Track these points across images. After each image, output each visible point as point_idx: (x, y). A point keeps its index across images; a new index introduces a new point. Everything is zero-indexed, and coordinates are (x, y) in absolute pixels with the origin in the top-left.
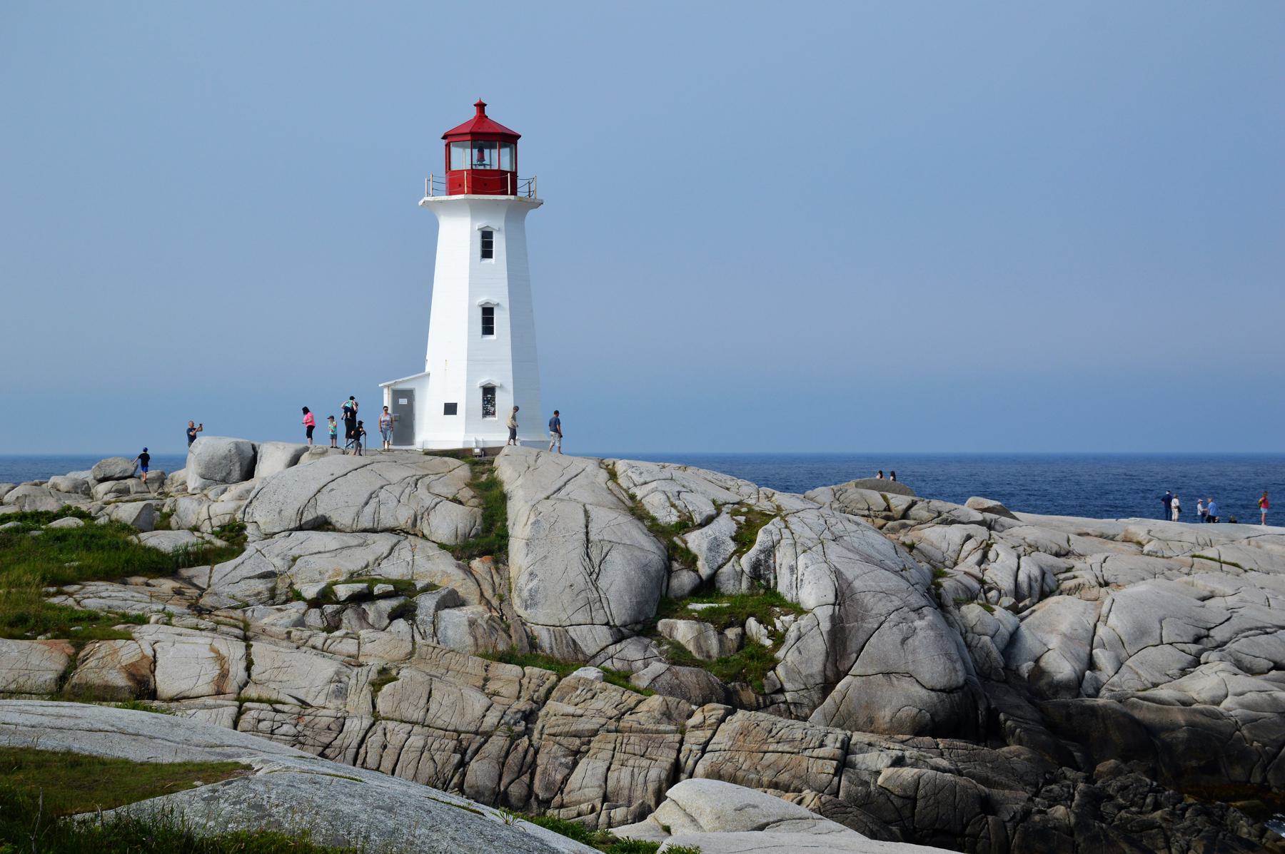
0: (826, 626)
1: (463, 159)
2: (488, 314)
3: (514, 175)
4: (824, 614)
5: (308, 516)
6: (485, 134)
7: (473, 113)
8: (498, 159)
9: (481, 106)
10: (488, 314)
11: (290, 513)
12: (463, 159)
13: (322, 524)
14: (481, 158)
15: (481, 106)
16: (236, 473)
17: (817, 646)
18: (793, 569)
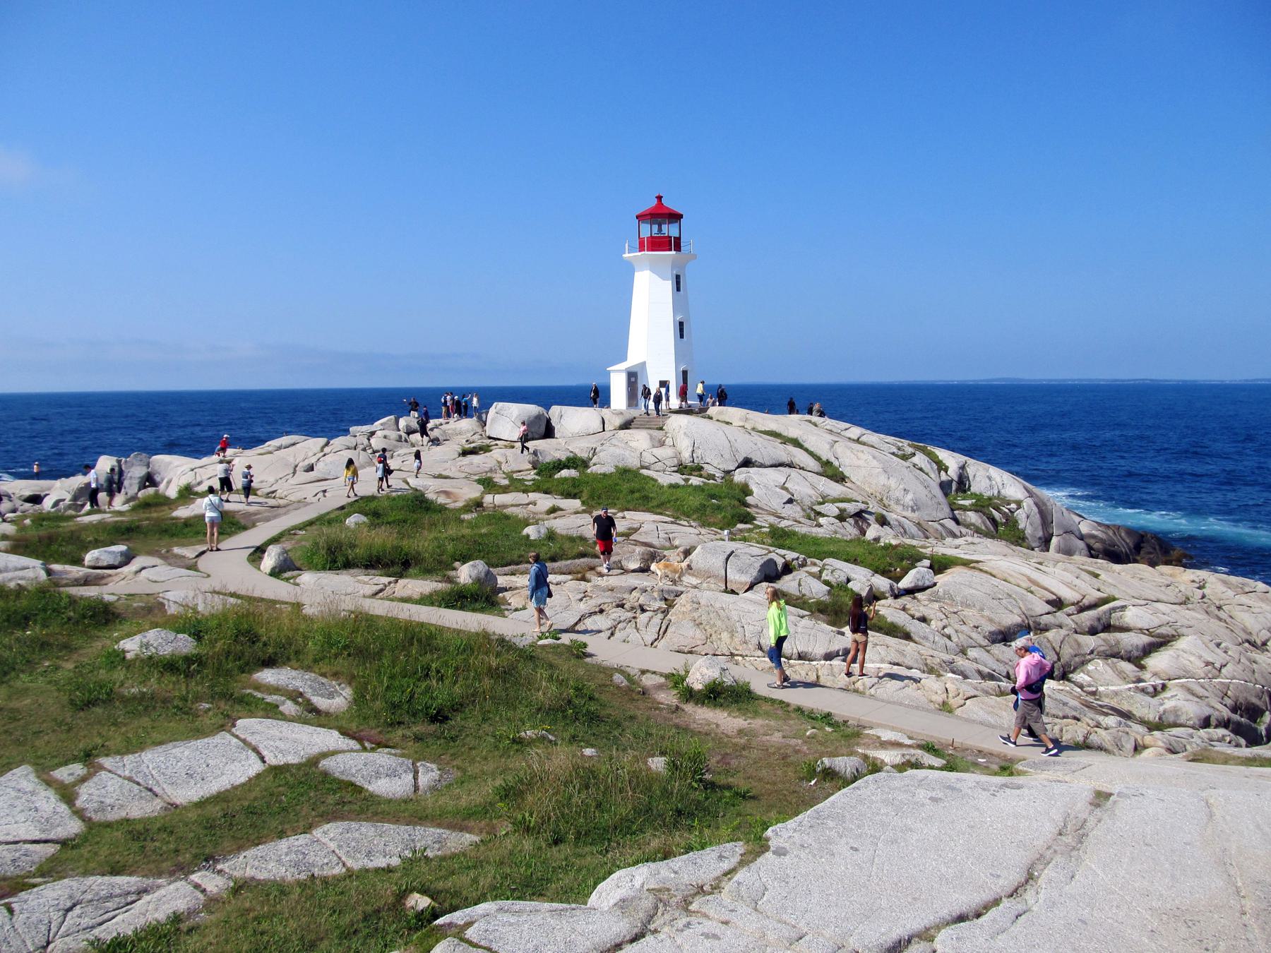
0: (1035, 509)
1: (647, 230)
2: (681, 324)
3: (678, 240)
4: (1030, 501)
5: (740, 460)
6: (661, 214)
7: (655, 202)
8: (670, 230)
9: (659, 198)
10: (681, 324)
11: (727, 456)
12: (647, 230)
13: (747, 463)
14: (660, 230)
15: (659, 198)
16: (543, 429)
17: (1037, 518)
18: (990, 478)
